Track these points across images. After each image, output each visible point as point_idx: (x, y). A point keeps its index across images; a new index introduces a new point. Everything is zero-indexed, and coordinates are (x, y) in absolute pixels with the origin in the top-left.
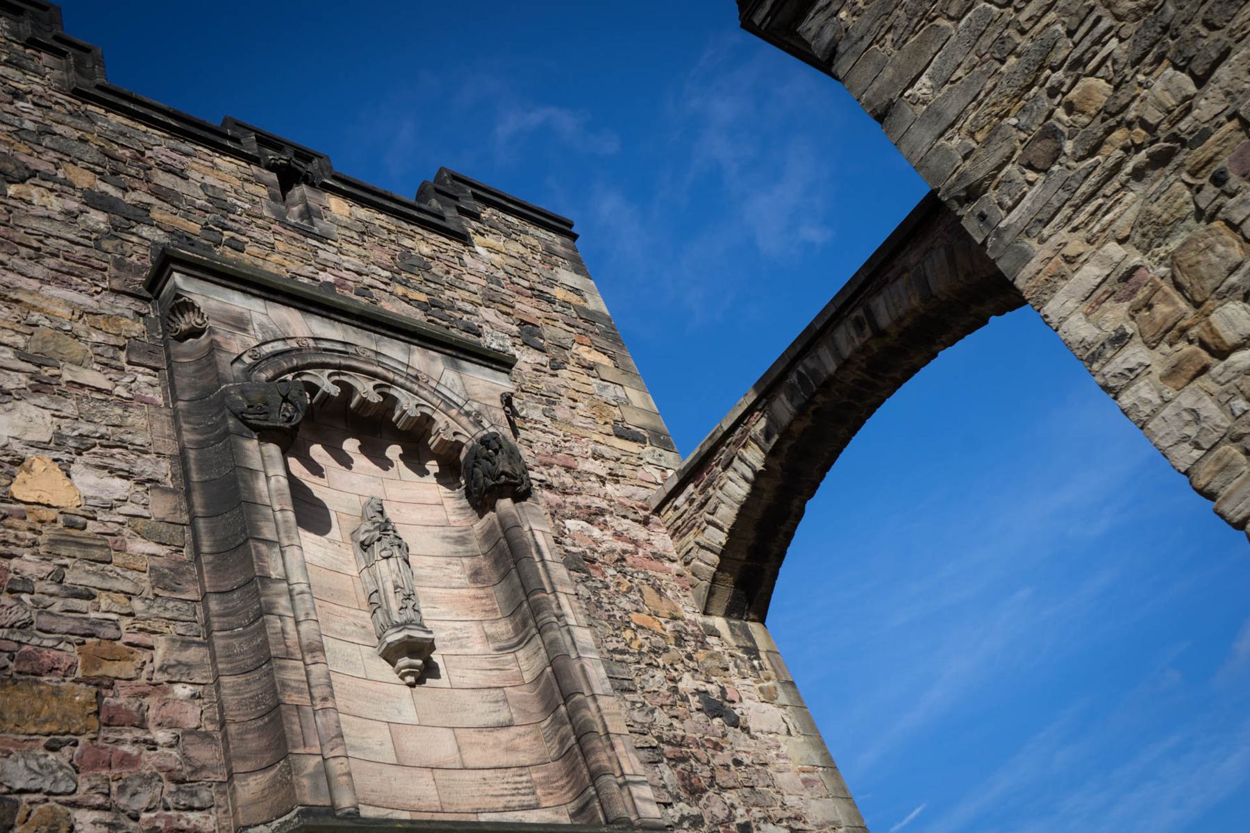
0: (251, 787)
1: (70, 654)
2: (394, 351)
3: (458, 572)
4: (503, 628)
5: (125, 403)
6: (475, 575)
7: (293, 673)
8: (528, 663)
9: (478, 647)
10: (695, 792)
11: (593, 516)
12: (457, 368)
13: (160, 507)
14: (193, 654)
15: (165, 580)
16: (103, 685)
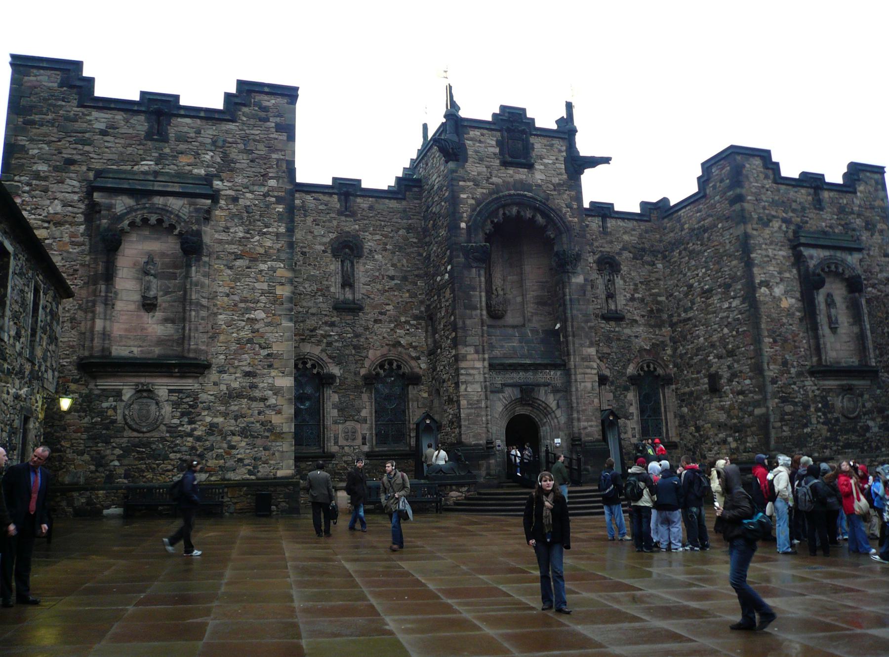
0: (815, 359)
1: (790, 337)
2: (839, 254)
3: (844, 307)
4: (851, 320)
5: (792, 280)
6: (847, 307)
7: (821, 342)
8: (856, 329)
9: (846, 324)
10: (881, 355)
11: (873, 286)
12: (851, 254)
13: (800, 304)
14: (805, 334)
15: (801, 320)
16: (795, 341)
